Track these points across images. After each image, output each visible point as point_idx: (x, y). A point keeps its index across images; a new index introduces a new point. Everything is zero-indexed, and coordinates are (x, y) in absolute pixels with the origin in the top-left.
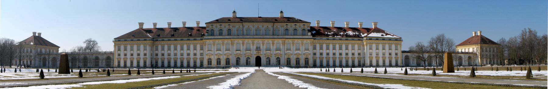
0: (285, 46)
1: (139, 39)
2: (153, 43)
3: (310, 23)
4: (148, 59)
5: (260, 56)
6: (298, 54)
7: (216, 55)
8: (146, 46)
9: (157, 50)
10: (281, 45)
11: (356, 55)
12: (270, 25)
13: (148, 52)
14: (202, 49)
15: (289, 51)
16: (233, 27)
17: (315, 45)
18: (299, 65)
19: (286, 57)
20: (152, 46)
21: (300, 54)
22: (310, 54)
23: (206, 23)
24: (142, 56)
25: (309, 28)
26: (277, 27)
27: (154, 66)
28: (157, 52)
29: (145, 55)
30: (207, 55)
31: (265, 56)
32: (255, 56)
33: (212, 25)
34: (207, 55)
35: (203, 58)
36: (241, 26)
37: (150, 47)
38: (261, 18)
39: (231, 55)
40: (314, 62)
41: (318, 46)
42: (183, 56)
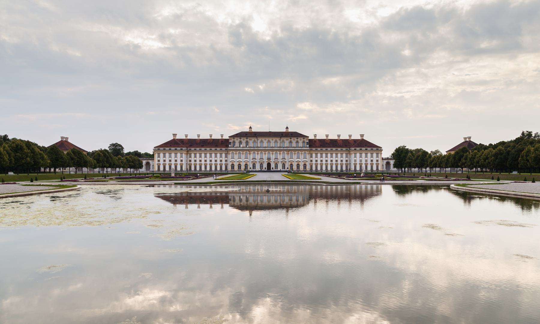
0: (288, 155)
1: (181, 148)
2: (187, 151)
4: (184, 165)
5: (270, 163)
7: (238, 162)
8: (182, 155)
9: (190, 157)
10: (286, 154)
11: (344, 162)
12: (278, 139)
13: (184, 158)
14: (226, 157)
15: (292, 160)
16: (250, 140)
17: (312, 154)
18: (299, 170)
19: (290, 163)
20: (187, 154)
21: (300, 162)
22: (307, 162)
23: (229, 137)
24: (179, 162)
25: (308, 141)
26: (283, 140)
27: (188, 170)
28: (190, 159)
29: (182, 161)
30: (231, 162)
31: (274, 163)
32: (267, 163)
33: (234, 138)
34: (231, 162)
35: (228, 164)
36: (256, 140)
37: (186, 155)
38: (271, 133)
39: (248, 162)
40: (311, 167)
41: (314, 155)
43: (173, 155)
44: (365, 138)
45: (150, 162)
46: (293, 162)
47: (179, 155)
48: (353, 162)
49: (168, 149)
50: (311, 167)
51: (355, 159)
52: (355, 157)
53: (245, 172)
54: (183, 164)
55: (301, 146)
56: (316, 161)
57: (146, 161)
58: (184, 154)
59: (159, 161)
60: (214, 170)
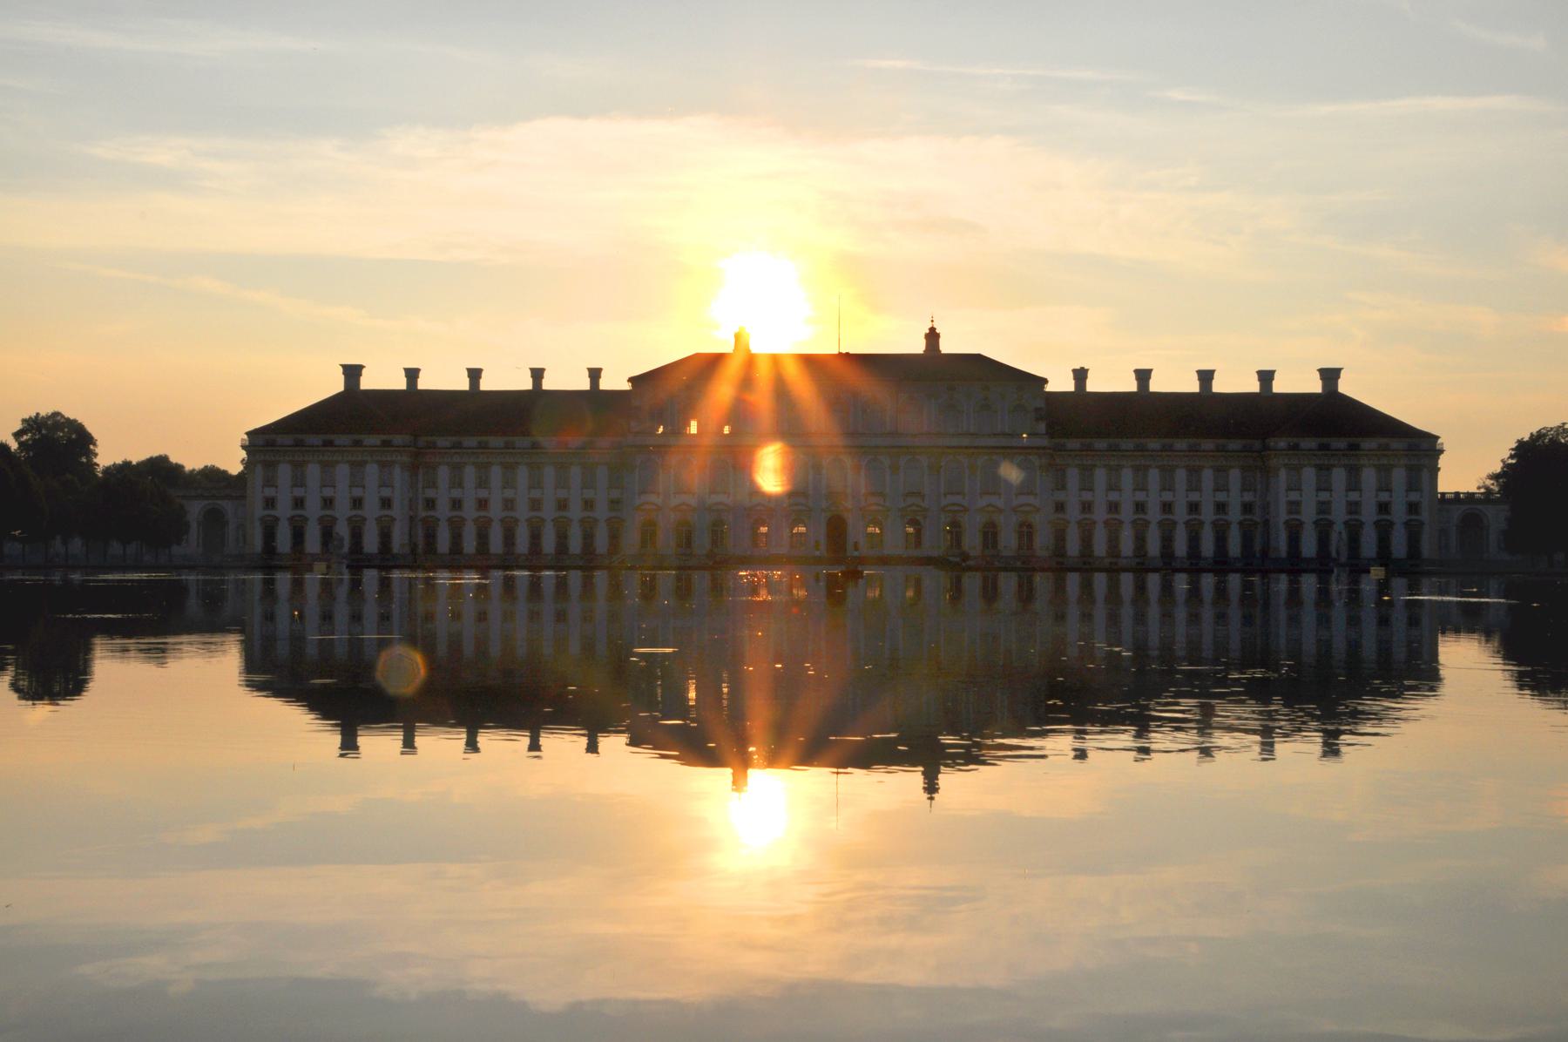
3: (1045, 381)
6: (991, 509)
11: (1235, 515)
20: (413, 469)
21: (1000, 511)
23: (631, 380)
24: (371, 510)
29: (386, 503)
41: (1073, 476)
42: (539, 509)
43: (343, 471)
44: (1345, 387)
45: (228, 506)
46: (966, 510)
47: (372, 471)
48: (1281, 516)
49: (315, 440)
50: (1060, 537)
51: (1294, 496)
52: (1295, 487)
53: (711, 563)
54: (393, 519)
55: (1007, 430)
56: (1087, 507)
57: (206, 502)
58: (397, 471)
59: (270, 503)
60: (553, 552)
